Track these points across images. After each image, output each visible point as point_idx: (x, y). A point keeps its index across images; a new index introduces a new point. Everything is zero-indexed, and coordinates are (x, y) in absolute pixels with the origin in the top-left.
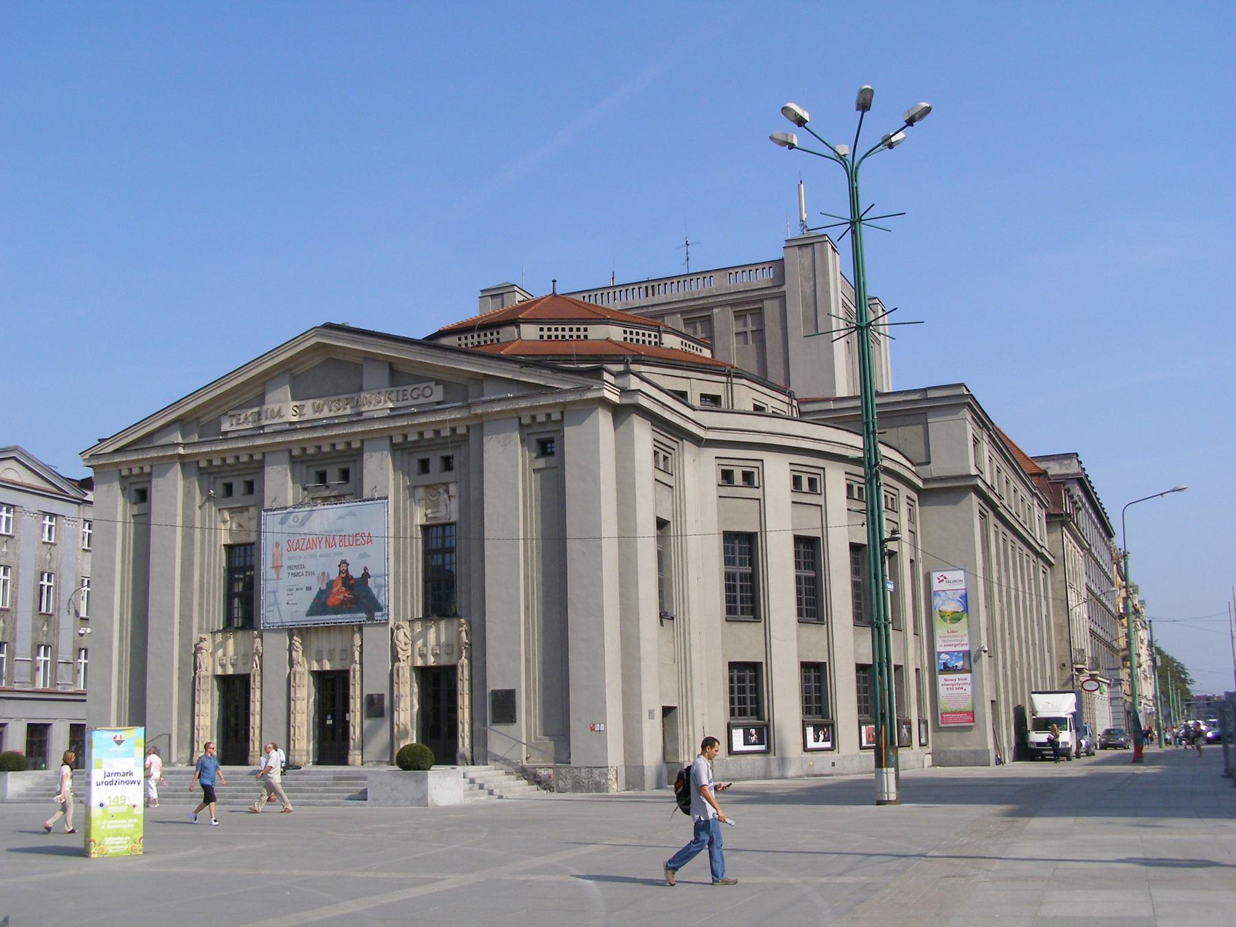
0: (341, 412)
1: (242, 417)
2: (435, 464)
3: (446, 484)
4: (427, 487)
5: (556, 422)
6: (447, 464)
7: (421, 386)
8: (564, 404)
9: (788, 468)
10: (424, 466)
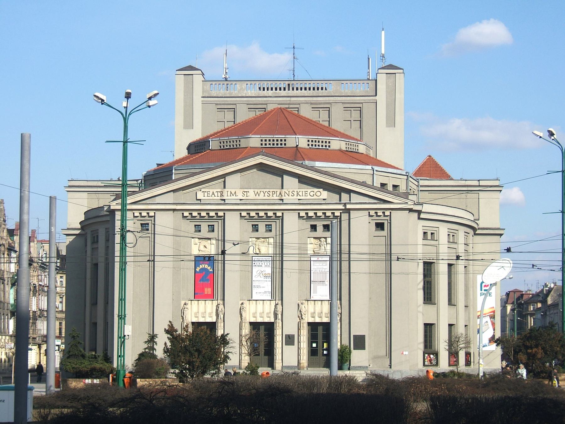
0: (271, 197)
1: (211, 193)
2: (320, 228)
7: (316, 190)
9: (447, 230)
10: (314, 228)
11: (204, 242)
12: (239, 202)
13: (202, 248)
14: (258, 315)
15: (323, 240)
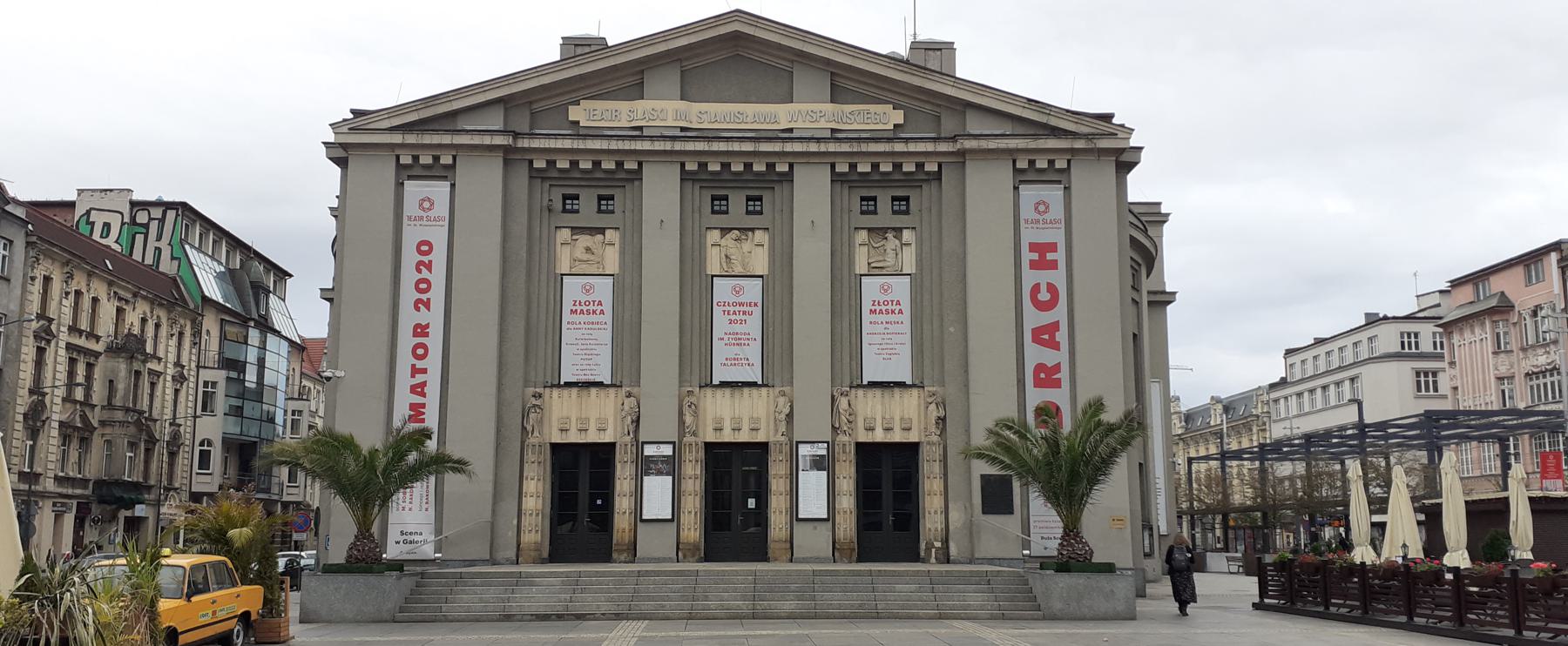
2: (884, 203)
3: (898, 231)
4: (869, 230)
5: (1061, 171)
6: (901, 204)
8: (1073, 151)
11: (584, 240)
12: (678, 133)
13: (580, 253)
14: (727, 426)
15: (890, 235)
